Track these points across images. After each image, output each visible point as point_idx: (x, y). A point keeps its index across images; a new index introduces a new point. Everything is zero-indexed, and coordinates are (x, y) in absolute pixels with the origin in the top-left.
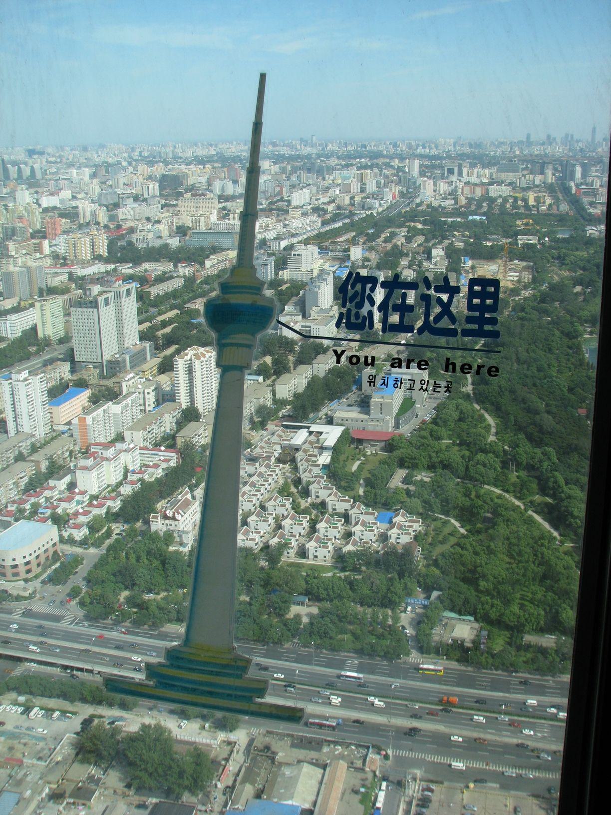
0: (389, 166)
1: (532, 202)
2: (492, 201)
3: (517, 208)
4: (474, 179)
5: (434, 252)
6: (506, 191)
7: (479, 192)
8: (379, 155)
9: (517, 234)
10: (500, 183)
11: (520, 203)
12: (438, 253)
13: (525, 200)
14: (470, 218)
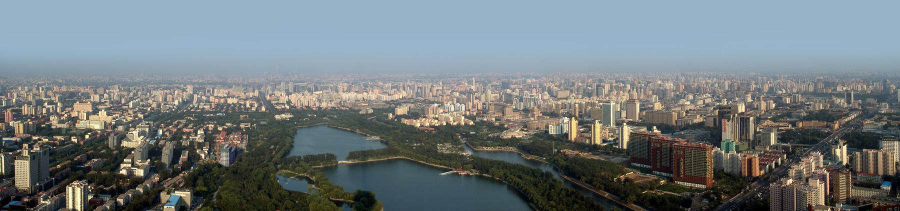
0: (178, 88)
1: (248, 106)
2: (229, 105)
3: (241, 109)
4: (220, 95)
5: (199, 132)
6: (235, 101)
7: (222, 101)
8: (174, 82)
10: (233, 97)
11: (242, 106)
13: (245, 105)
14: (218, 114)
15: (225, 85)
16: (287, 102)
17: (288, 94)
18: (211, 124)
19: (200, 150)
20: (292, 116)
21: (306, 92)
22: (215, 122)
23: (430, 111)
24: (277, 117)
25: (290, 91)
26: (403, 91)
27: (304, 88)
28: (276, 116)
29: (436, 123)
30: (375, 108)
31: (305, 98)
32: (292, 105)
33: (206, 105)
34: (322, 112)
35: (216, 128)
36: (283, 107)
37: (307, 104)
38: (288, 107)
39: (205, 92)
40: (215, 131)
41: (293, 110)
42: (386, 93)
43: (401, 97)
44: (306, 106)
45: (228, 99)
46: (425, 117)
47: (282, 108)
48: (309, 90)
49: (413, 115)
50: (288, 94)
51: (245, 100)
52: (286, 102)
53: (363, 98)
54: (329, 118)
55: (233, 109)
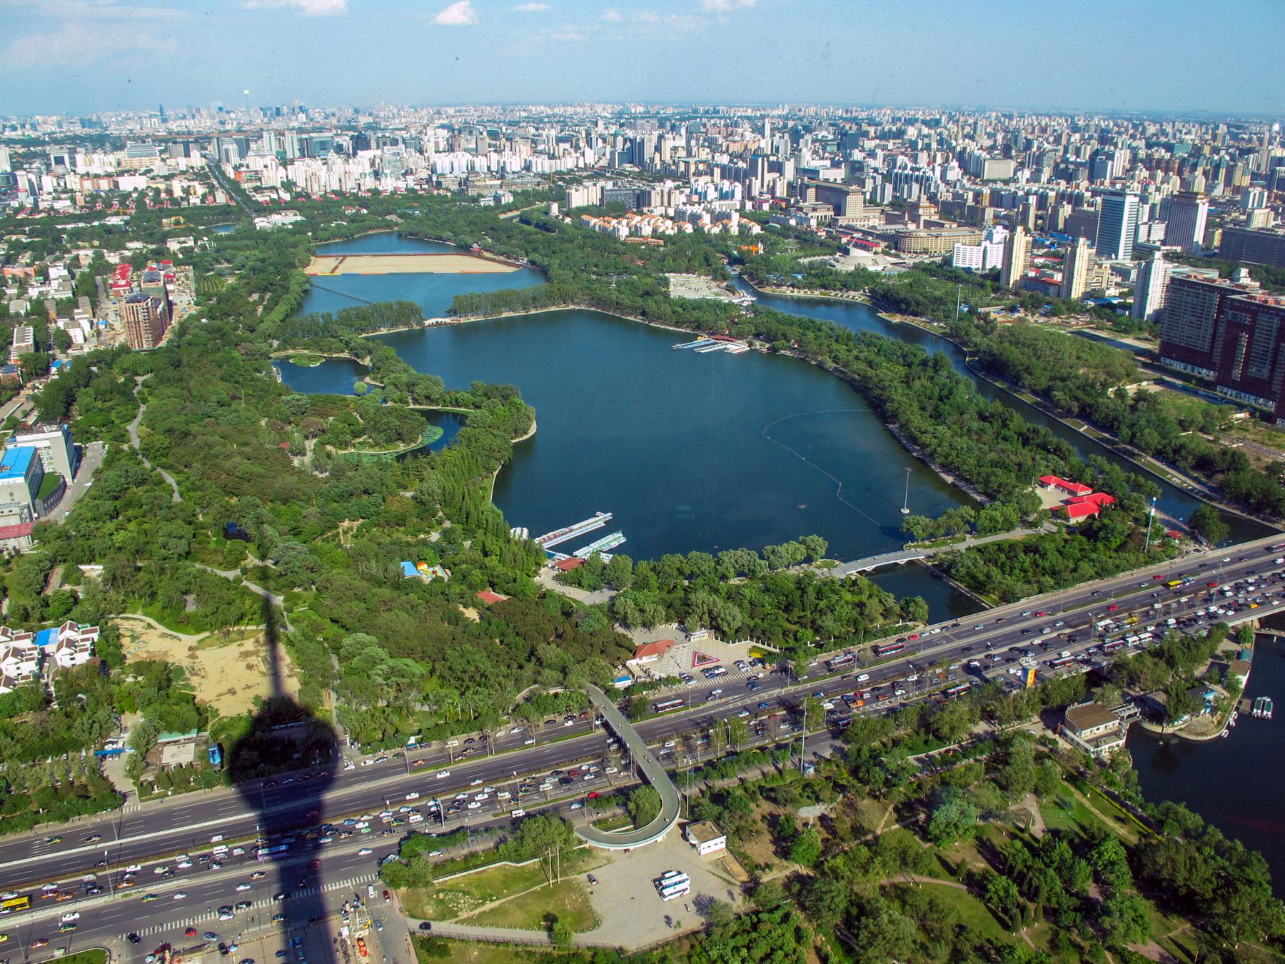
4: (95, 170)
5: (53, 272)
6: (141, 182)
7: (105, 185)
9: (164, 237)
10: (132, 172)
11: (163, 195)
12: (57, 272)
13: (169, 192)
15: (100, 142)
16: (283, 183)
17: (285, 162)
18: (84, 248)
19: (67, 320)
20: (299, 218)
21: (332, 156)
22: (96, 243)
23: (655, 198)
24: (261, 223)
25: (290, 156)
26: (587, 150)
27: (324, 145)
28: (257, 220)
29: (669, 228)
30: (519, 190)
31: (329, 170)
32: (299, 190)
33: (60, 199)
34: (381, 202)
35: (99, 256)
36: (275, 196)
37: (336, 187)
38: (286, 196)
39: (48, 165)
40: (100, 266)
41: (301, 201)
42: (541, 153)
43: (581, 165)
44: (333, 192)
45: (120, 180)
46: (641, 213)
47: (272, 201)
48: (339, 149)
49: (610, 208)
50: (285, 162)
51: (168, 178)
52: (279, 185)
53: (489, 168)
54: (401, 216)
55: (140, 202)
